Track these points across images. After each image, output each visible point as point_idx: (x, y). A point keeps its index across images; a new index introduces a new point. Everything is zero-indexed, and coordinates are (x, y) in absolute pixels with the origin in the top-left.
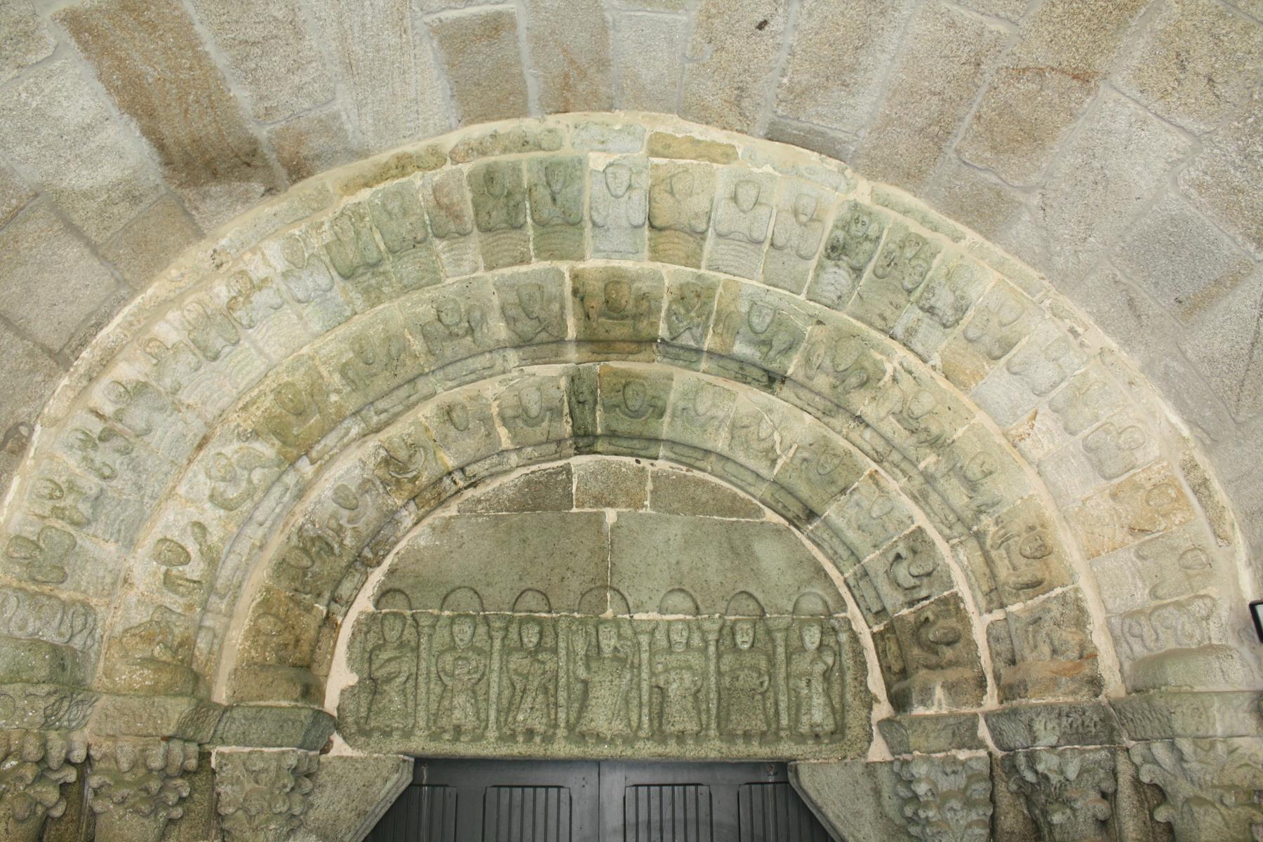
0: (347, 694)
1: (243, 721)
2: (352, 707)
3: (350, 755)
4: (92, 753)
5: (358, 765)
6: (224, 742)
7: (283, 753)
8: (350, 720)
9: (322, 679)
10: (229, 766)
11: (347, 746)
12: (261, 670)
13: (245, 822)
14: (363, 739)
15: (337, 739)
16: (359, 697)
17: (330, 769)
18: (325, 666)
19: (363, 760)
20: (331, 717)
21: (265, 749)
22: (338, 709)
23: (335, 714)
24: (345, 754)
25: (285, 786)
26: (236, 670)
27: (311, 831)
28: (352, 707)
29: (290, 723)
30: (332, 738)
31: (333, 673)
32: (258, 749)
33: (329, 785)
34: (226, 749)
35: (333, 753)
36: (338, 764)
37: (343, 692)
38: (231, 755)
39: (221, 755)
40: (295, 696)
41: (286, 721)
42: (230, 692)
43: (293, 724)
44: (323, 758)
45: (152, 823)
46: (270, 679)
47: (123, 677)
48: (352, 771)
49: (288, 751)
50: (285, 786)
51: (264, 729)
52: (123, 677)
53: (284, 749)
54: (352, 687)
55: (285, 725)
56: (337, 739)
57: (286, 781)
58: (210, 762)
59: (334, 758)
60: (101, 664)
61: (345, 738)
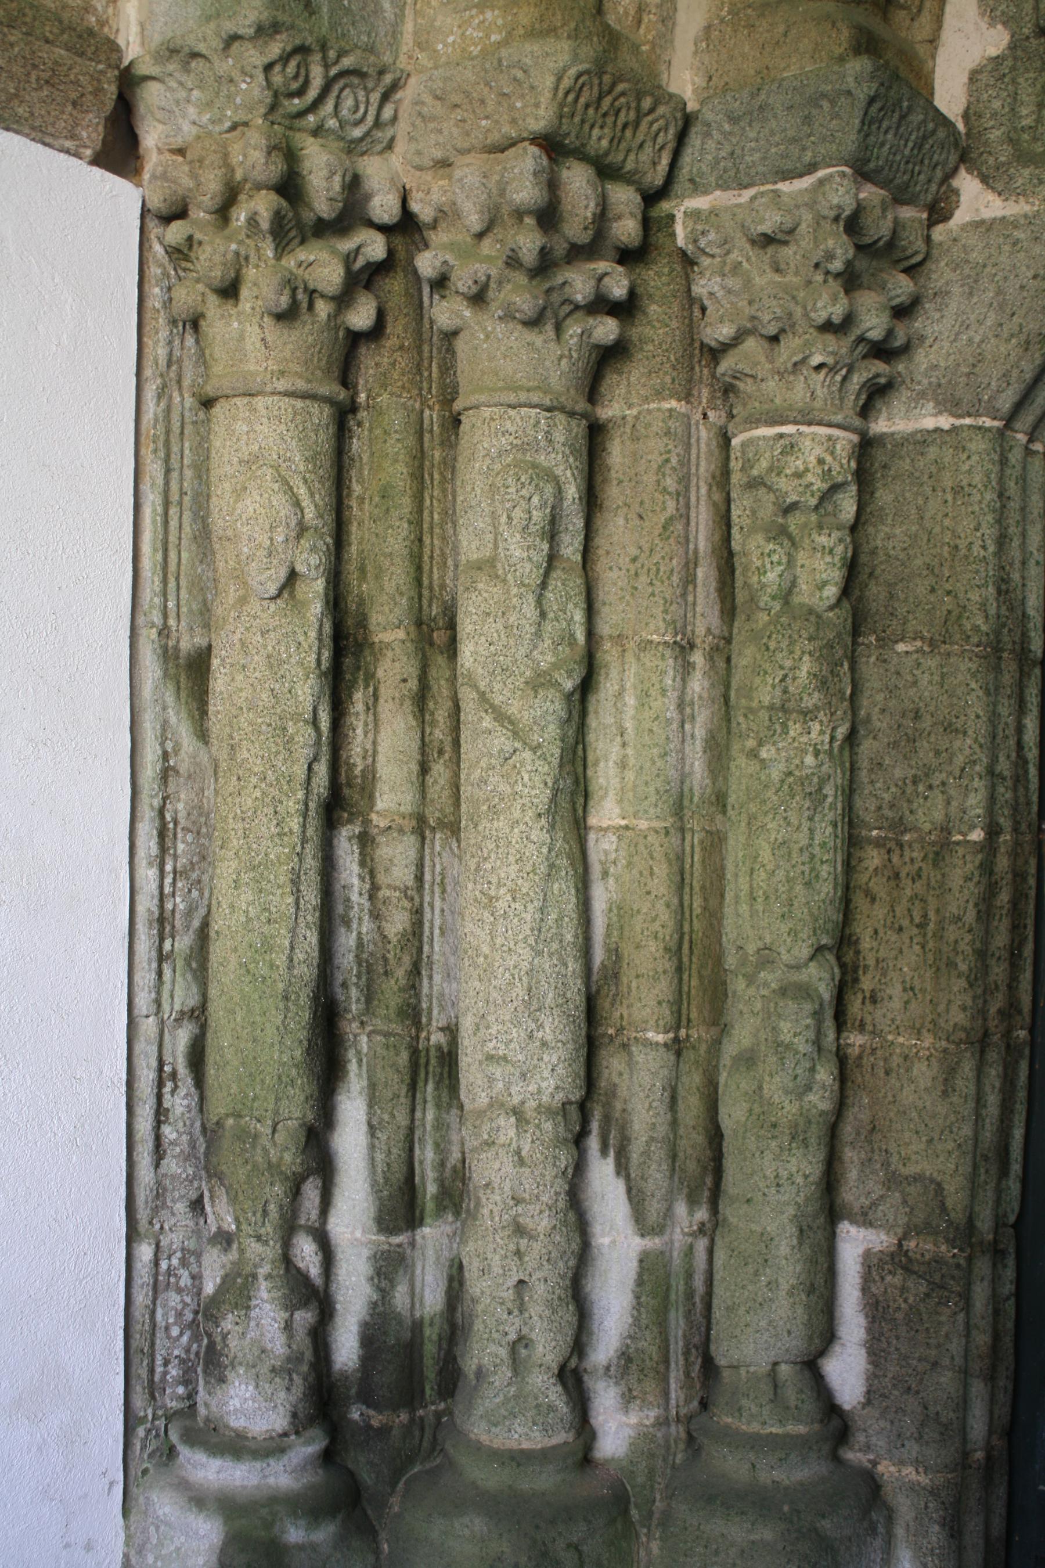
0: (984, 77)
1: (727, 127)
2: (997, 104)
3: (999, 214)
4: (415, 207)
5: (1018, 234)
6: (697, 187)
7: (821, 182)
8: (995, 135)
9: (922, 50)
10: (712, 236)
11: (991, 196)
12: (762, 15)
13: (763, 359)
14: (1026, 172)
15: (967, 184)
16: (1014, 81)
17: (956, 252)
18: (925, 18)
19: (1030, 220)
20: (944, 121)
21: (784, 187)
22: (966, 116)
23: (961, 126)
24: (987, 214)
25: (830, 256)
26: (708, 28)
27: (922, 395)
28: (997, 104)
29: (826, 104)
30: (955, 183)
31: (948, 35)
32: (770, 187)
33: (956, 290)
34: (701, 203)
35: (961, 216)
36: (972, 239)
37: (974, 76)
38: (714, 212)
39: (694, 215)
40: (838, 51)
41: (814, 101)
42: (701, 81)
43: (833, 103)
44: (939, 233)
45: (552, 345)
46: (781, 28)
47: (451, 39)
48: (1007, 248)
49: (831, 176)
50: (830, 256)
51: (772, 133)
52: (451, 39)
53: (821, 173)
54: (997, 60)
55: (814, 112)
56: (967, 184)
57: (830, 243)
58: (673, 235)
59: (963, 228)
60: (409, 27)
61: (985, 179)
